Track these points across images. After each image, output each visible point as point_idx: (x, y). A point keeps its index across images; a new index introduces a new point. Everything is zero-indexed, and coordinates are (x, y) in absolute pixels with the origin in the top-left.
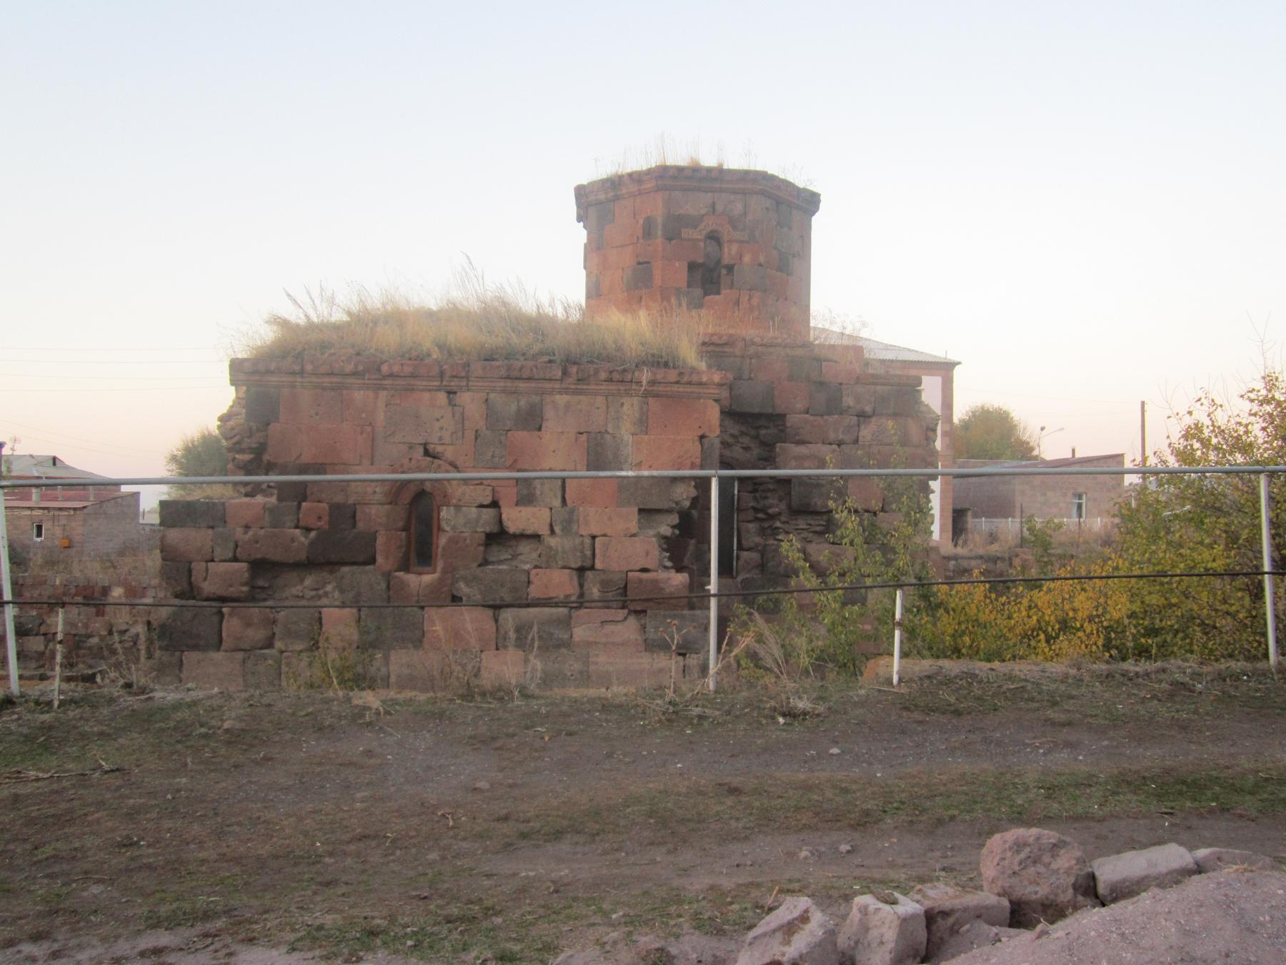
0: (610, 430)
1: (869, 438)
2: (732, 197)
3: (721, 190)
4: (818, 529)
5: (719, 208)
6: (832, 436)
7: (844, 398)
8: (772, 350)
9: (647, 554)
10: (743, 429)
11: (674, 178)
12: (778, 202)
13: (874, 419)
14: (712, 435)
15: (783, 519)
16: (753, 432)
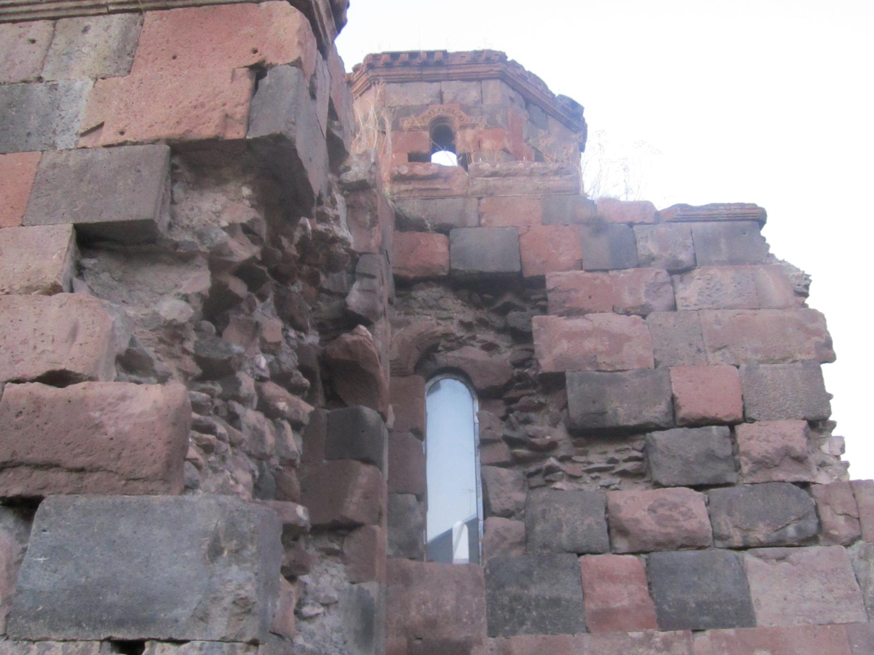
0: (46, 76)
1: (693, 300)
2: (465, 85)
3: (449, 78)
4: (629, 466)
5: (448, 97)
6: (628, 300)
7: (640, 244)
8: (510, 182)
9: (74, 333)
10: (482, 314)
11: (388, 65)
12: (529, 101)
13: (696, 273)
14: (280, 62)
15: (561, 453)
16: (498, 321)
